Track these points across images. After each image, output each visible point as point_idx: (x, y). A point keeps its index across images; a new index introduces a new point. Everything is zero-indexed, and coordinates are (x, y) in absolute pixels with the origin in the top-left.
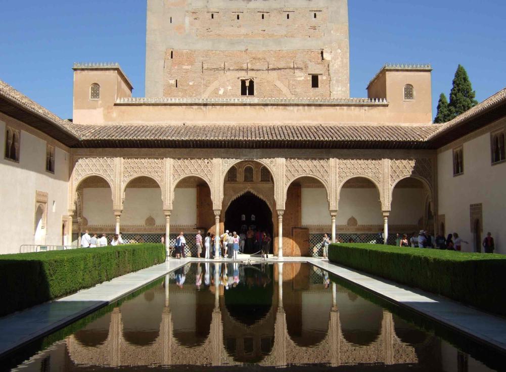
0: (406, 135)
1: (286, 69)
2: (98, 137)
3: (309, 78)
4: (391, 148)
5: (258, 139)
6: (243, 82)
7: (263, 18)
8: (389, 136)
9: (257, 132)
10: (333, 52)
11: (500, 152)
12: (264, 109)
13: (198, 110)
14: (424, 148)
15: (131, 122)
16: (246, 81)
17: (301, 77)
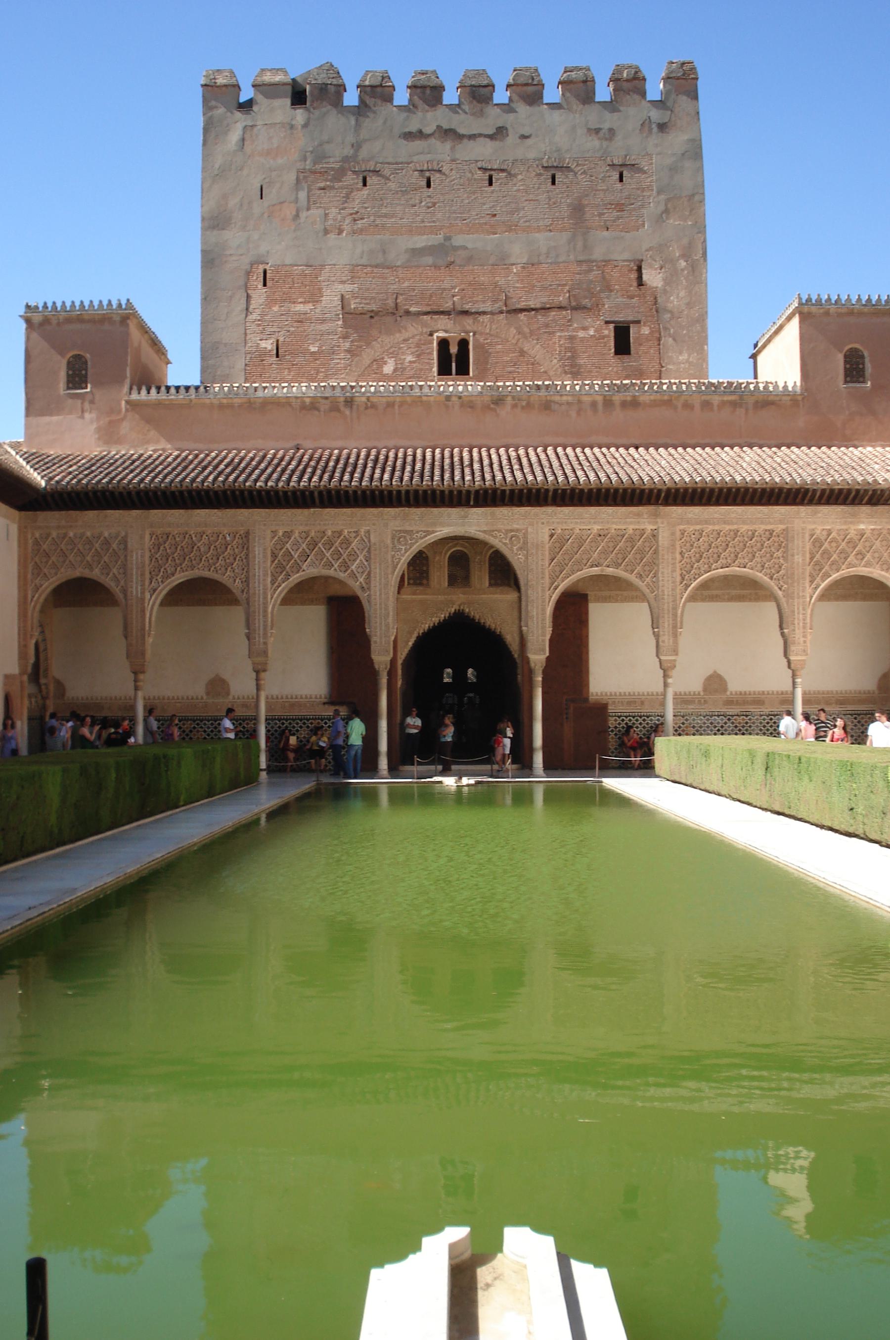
4: (810, 503)
6: (444, 344)
7: (491, 184)
9: (476, 466)
12: (495, 410)
16: (450, 340)
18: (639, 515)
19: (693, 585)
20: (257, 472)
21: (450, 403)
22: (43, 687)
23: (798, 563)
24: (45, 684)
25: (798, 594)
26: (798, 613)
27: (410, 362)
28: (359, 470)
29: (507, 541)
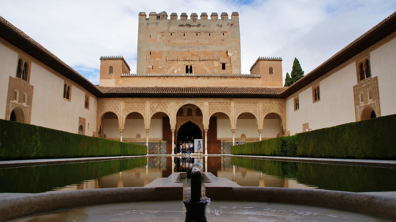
1: (209, 60)
3: (220, 65)
5: (194, 92)
6: (187, 67)
7: (197, 35)
8: (262, 92)
9: (194, 90)
11: (317, 96)
13: (164, 79)
14: (279, 98)
17: (217, 64)
18: (228, 100)
20: (148, 90)
21: (188, 78)
22: (102, 136)
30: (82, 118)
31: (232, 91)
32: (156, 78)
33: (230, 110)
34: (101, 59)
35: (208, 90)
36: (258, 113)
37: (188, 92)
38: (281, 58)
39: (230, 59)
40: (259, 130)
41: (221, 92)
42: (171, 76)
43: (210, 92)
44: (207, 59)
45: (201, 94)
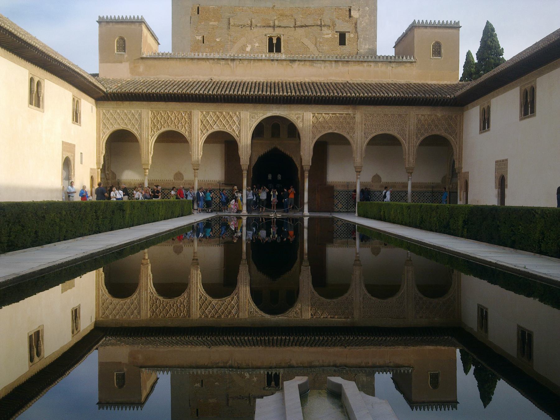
0: (434, 92)
1: (313, 26)
2: (124, 90)
3: (336, 36)
5: (285, 94)
6: (271, 39)
8: (416, 93)
9: (285, 88)
10: (361, 9)
12: (291, 66)
15: (158, 76)
16: (273, 37)
17: (329, 34)
18: (348, 109)
19: (369, 138)
20: (196, 88)
21: (273, 63)
23: (412, 129)
24: (108, 174)
25: (411, 142)
26: (411, 150)
27: (257, 46)
28: (237, 88)
29: (296, 119)
30: (68, 143)
31: (357, 91)
32: (211, 61)
33: (353, 128)
34: (99, 22)
35: (311, 88)
36: (407, 136)
37: (274, 94)
38: (459, 21)
39: (356, 24)
40: (407, 169)
41: (336, 94)
42: (240, 59)
43: (316, 93)
44: (310, 24)
45: (298, 98)
